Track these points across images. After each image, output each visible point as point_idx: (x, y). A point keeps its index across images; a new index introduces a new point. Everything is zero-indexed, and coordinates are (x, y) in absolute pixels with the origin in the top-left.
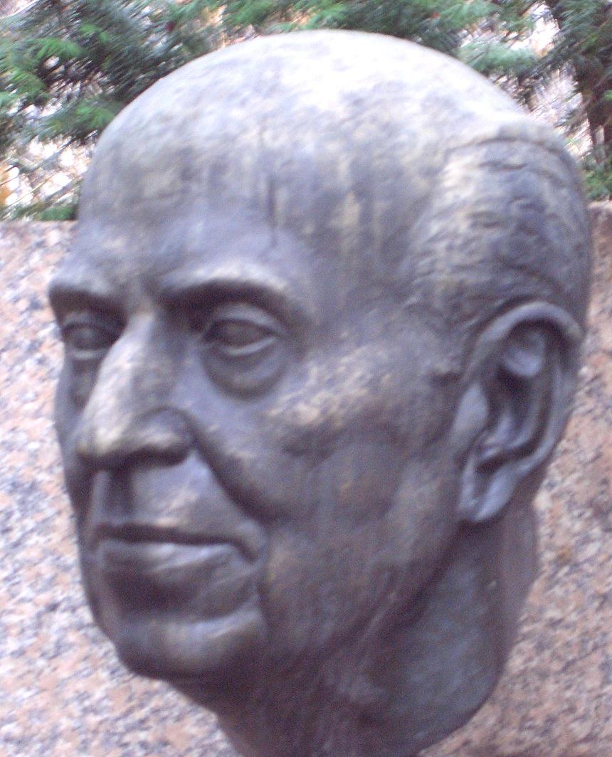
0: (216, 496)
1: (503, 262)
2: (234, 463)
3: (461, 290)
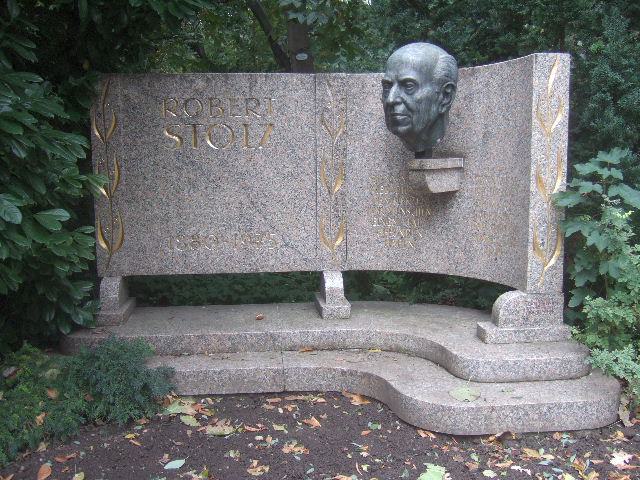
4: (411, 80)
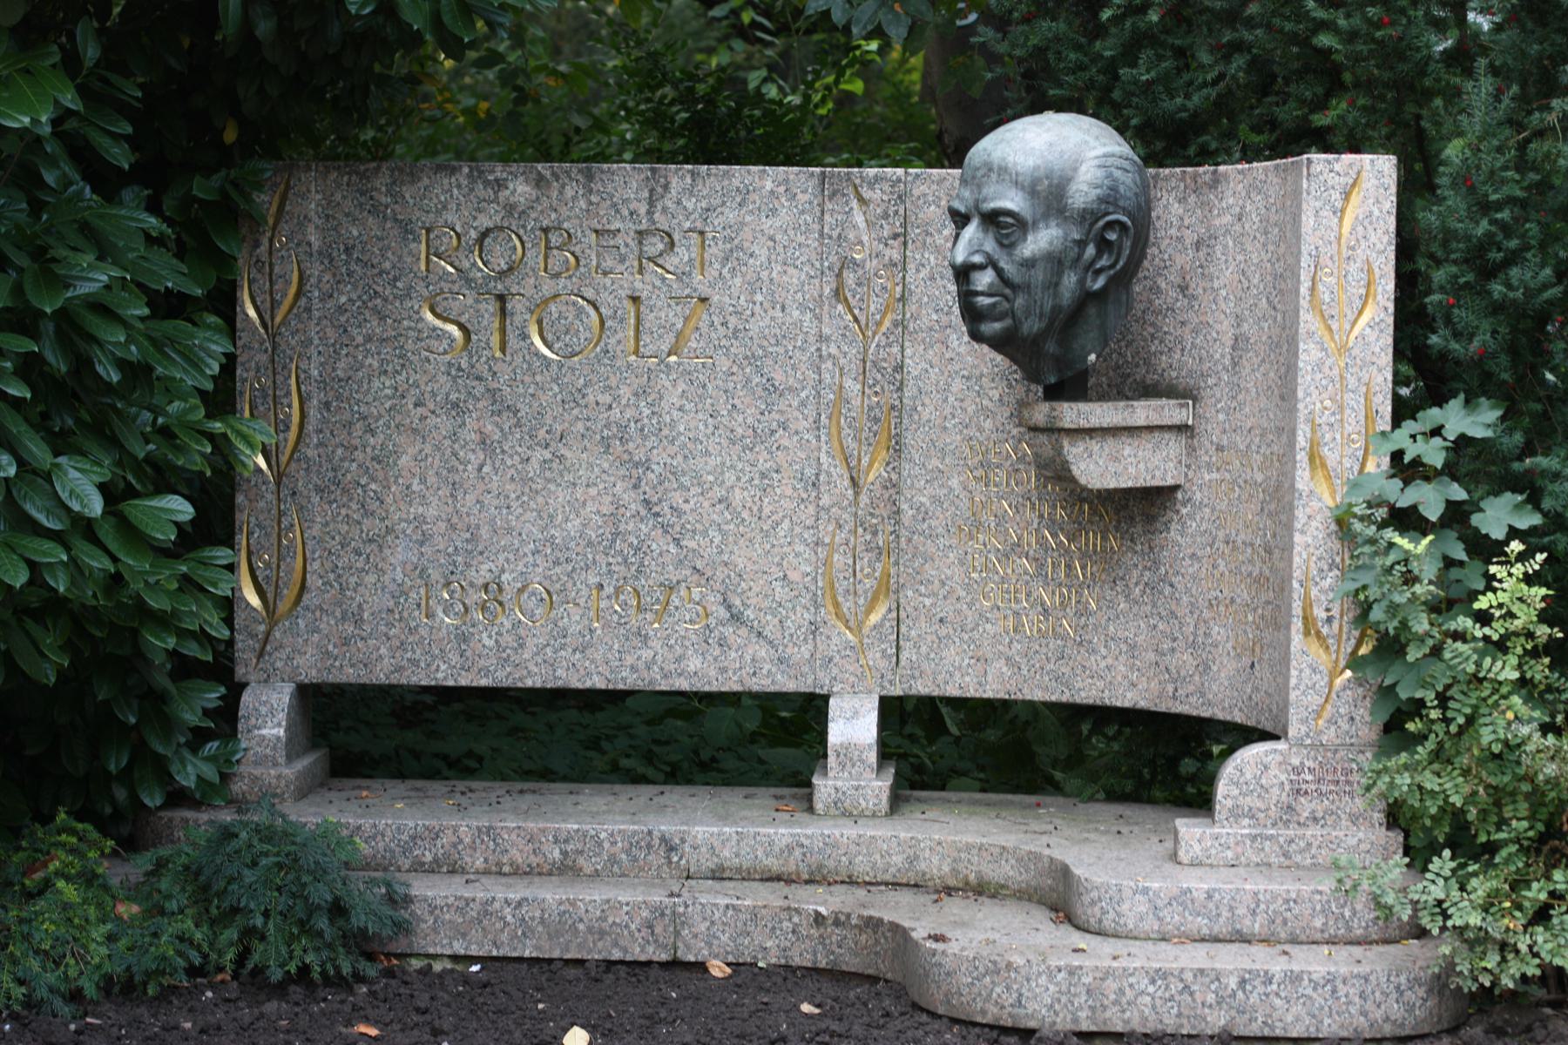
0: (997, 280)
1: (1102, 200)
2: (1002, 269)
3: (1084, 209)
4: (1009, 213)
